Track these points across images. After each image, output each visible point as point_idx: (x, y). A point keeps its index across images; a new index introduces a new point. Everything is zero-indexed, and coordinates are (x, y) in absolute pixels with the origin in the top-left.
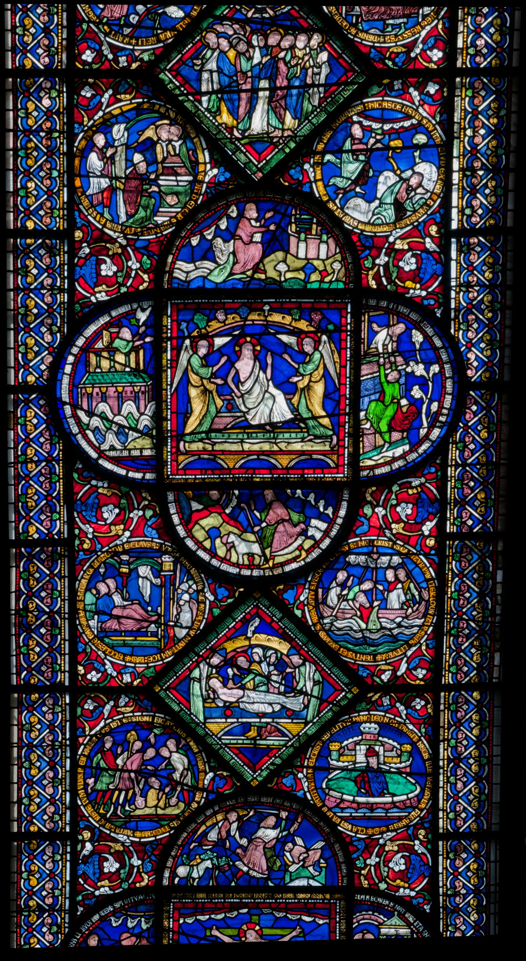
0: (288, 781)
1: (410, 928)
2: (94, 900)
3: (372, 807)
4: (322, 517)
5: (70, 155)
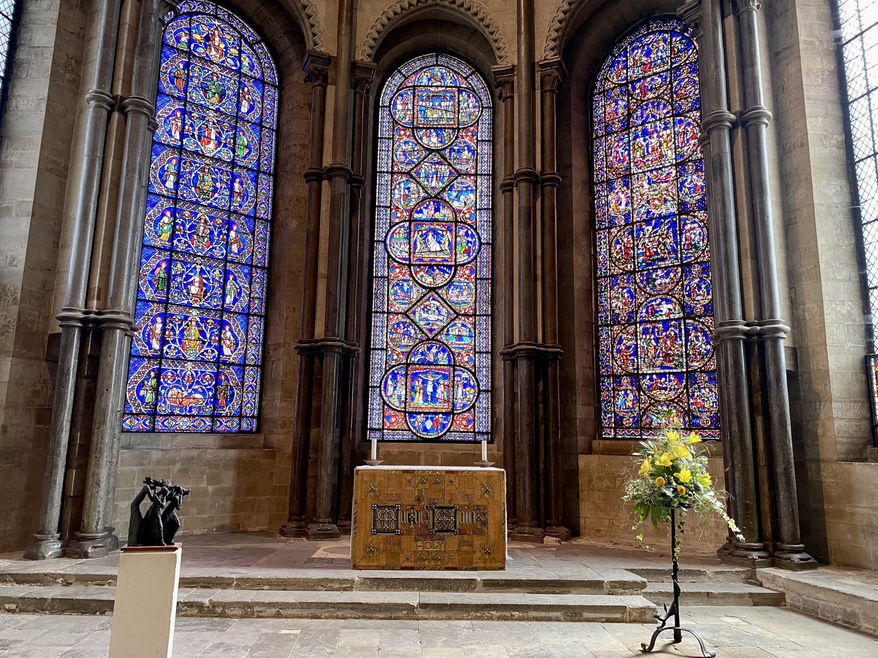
0: (439, 337)
3: (460, 345)
4: (448, 273)
5: (391, 190)
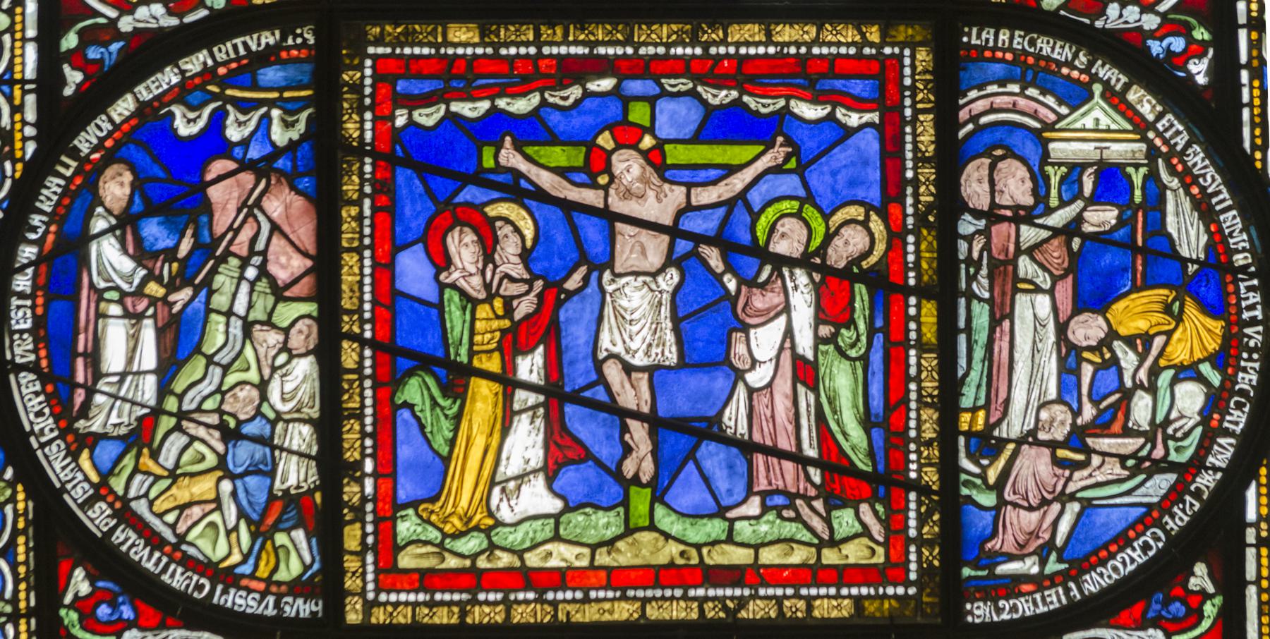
1: (1144, 139)
2: (115, 47)
